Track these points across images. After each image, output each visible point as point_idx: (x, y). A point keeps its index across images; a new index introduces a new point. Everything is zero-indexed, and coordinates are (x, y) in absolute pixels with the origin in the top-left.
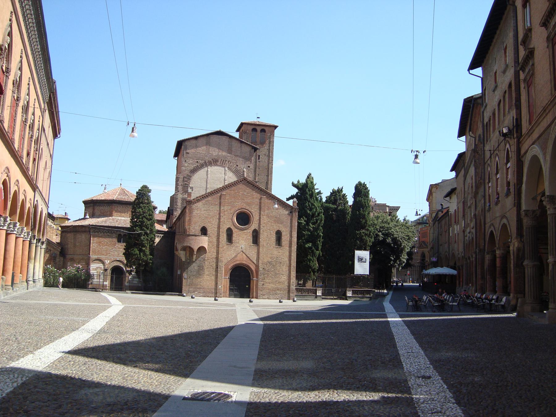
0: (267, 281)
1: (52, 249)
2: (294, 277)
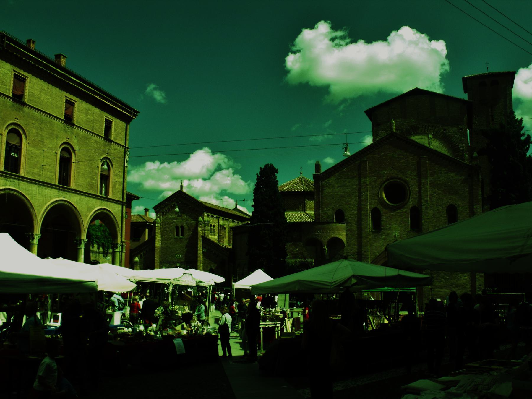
0: (437, 284)
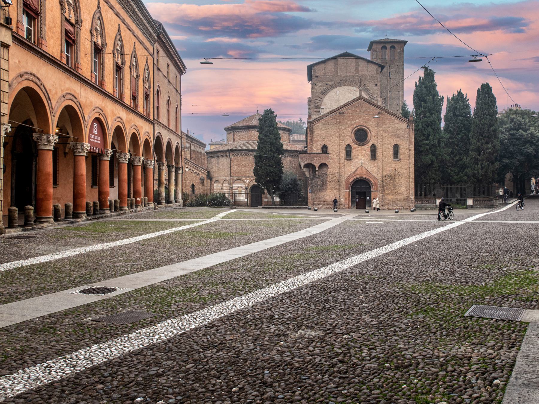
0: (387, 193)
1: (200, 173)
2: (412, 188)
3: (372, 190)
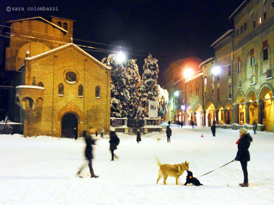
3: (79, 121)
